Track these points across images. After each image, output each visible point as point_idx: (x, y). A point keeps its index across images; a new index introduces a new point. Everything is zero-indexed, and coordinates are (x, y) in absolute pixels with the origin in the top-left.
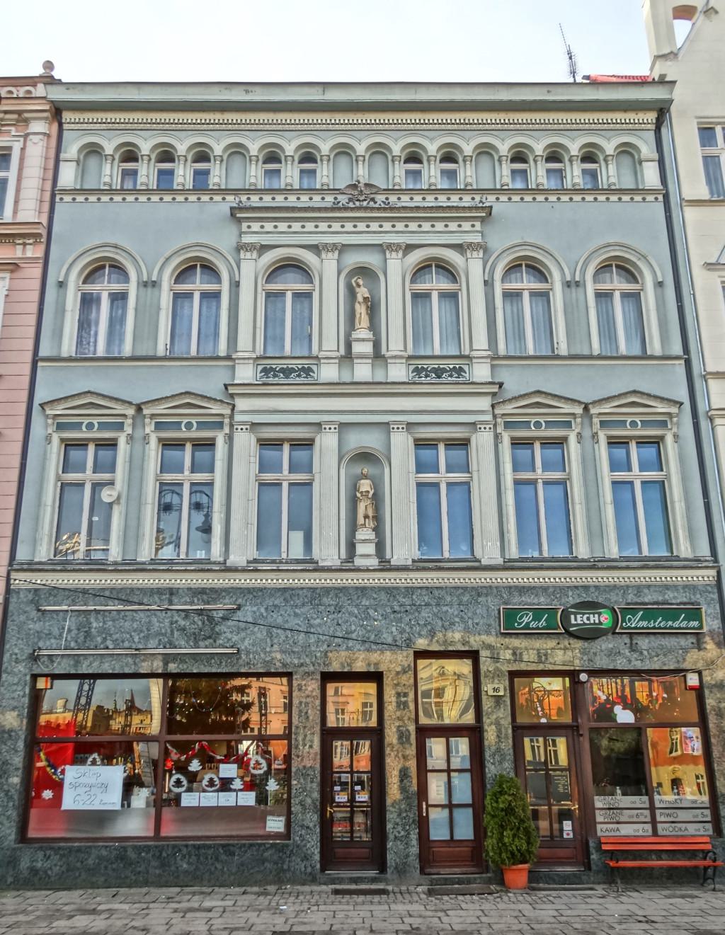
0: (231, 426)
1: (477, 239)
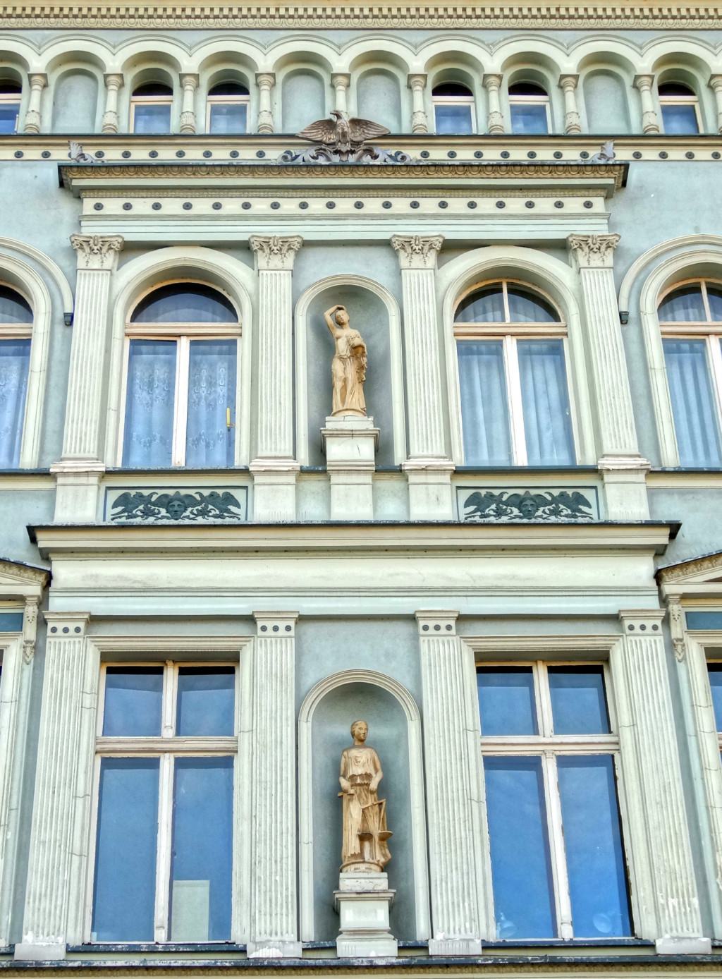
0: (42, 623)
1: (599, 229)
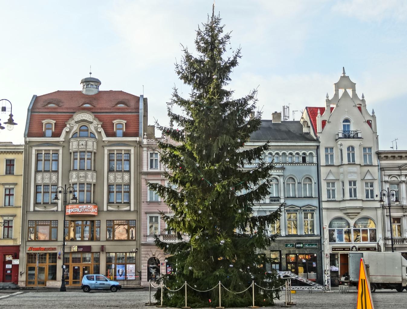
1: (282, 174)
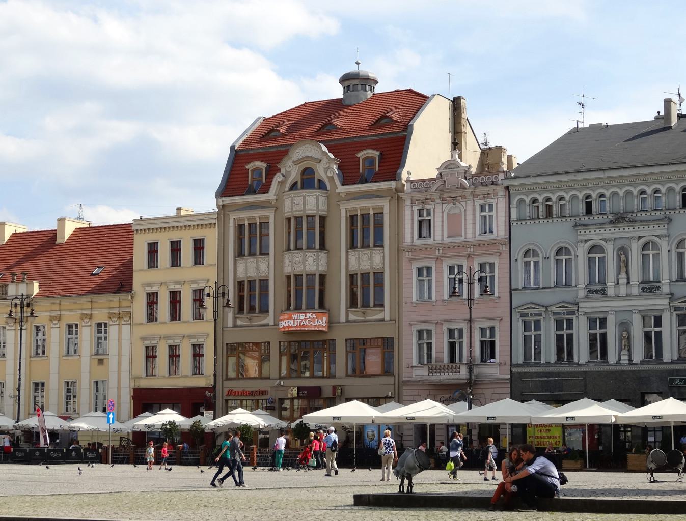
0: (578, 314)
1: (665, 232)
